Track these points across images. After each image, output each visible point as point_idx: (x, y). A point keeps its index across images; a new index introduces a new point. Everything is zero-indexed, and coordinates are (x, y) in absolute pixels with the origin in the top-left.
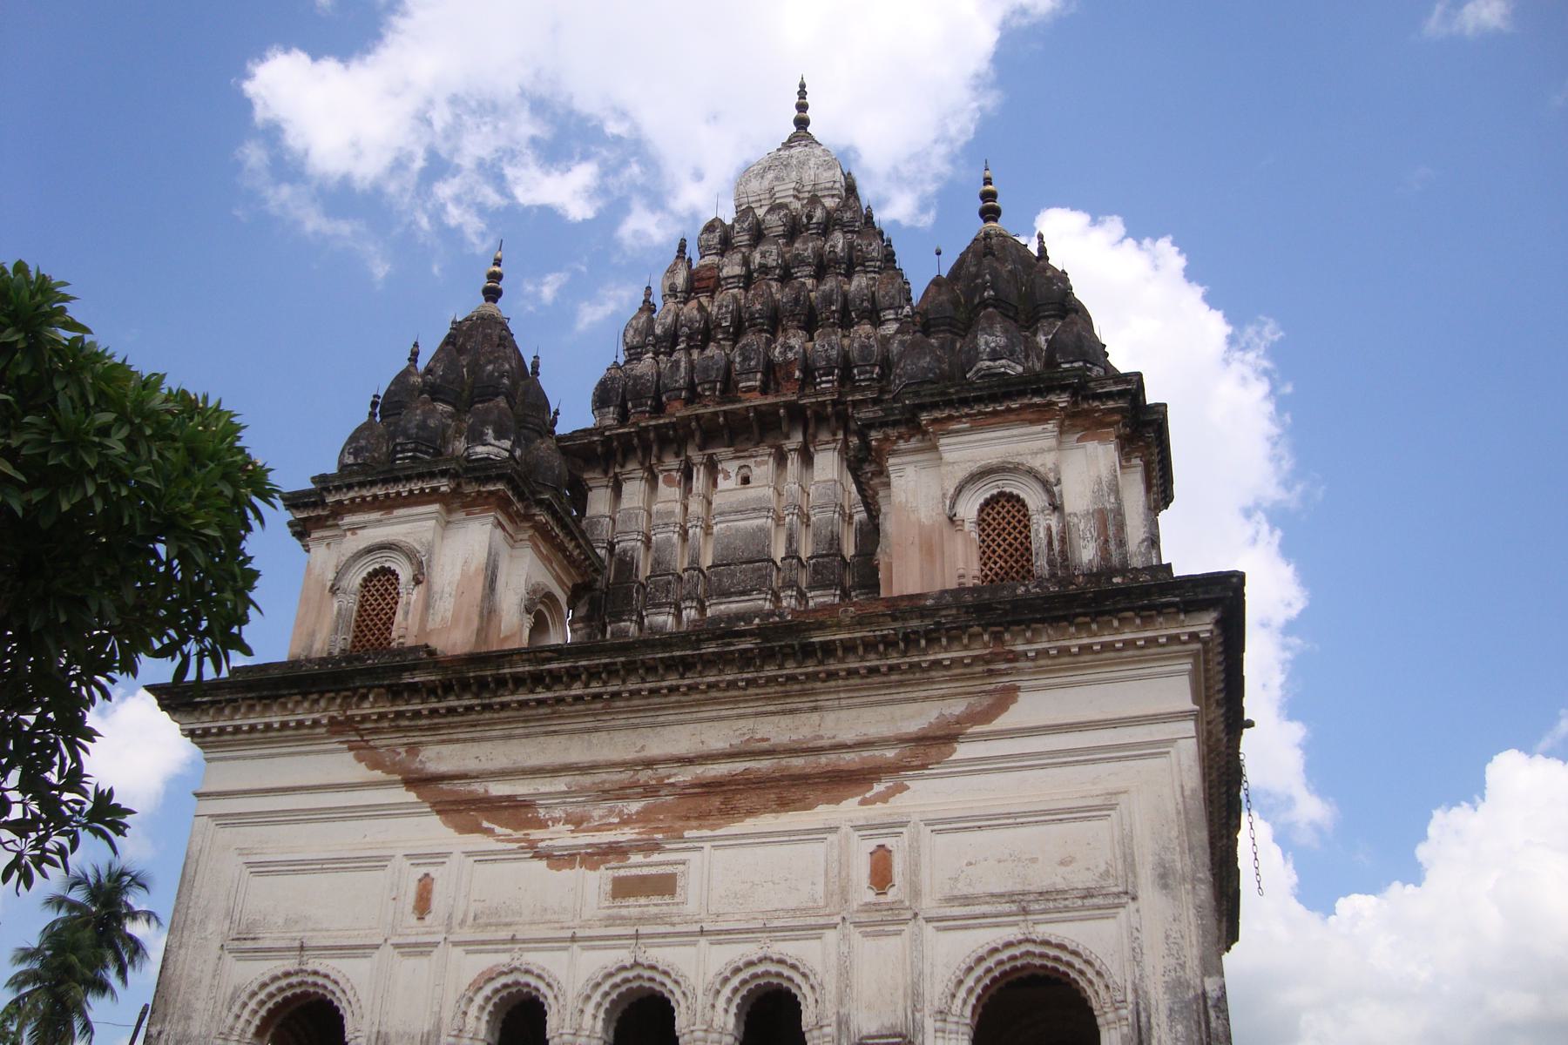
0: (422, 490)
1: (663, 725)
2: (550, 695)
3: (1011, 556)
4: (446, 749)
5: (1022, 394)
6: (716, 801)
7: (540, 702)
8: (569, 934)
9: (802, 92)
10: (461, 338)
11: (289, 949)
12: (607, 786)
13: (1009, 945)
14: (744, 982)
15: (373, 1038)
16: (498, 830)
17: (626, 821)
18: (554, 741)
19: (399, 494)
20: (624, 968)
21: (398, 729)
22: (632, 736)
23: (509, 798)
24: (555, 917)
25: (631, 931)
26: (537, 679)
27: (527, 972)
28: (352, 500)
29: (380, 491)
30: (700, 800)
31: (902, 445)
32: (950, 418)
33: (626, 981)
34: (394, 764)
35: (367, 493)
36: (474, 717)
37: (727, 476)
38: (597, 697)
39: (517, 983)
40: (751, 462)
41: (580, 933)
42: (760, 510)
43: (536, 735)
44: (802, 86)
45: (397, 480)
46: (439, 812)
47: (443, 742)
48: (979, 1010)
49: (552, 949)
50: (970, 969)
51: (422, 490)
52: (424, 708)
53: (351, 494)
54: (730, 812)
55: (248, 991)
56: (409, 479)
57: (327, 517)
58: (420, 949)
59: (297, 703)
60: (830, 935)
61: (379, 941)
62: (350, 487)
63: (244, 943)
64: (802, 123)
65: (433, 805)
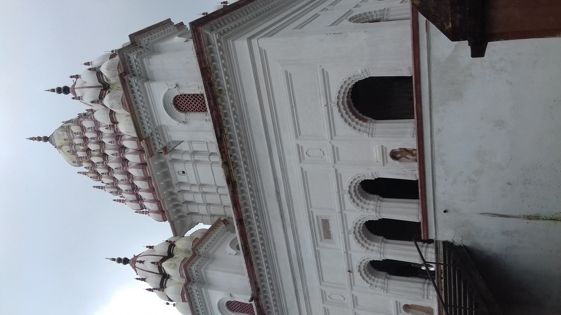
3: (197, 101)
9: (33, 139)
13: (340, 111)
14: (358, 198)
20: (356, 237)
27: (360, 266)
33: (360, 235)
39: (364, 269)
44: (31, 139)
48: (365, 117)
50: (349, 124)
60: (338, 172)
64: (46, 139)
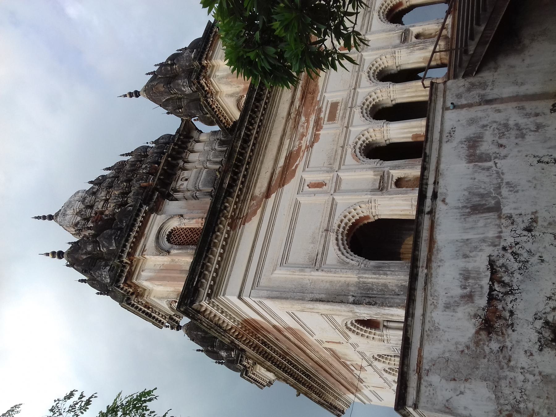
0: (143, 217)
1: (276, 113)
2: (252, 140)
4: (258, 185)
5: (209, 36)
6: (309, 96)
7: (254, 144)
8: (345, 129)
9: (38, 218)
10: (73, 263)
11: (326, 237)
12: (293, 126)
15: (372, 193)
16: (297, 163)
17: (308, 121)
18: (270, 146)
19: (139, 227)
21: (244, 201)
22: (277, 121)
23: (286, 158)
24: (337, 137)
25: (349, 109)
26: (246, 141)
28: (131, 247)
29: (133, 234)
30: (307, 100)
31: (208, 73)
32: (207, 55)
34: (257, 205)
35: (131, 239)
36: (250, 171)
37: (182, 184)
38: (259, 127)
40: (181, 177)
41: (346, 125)
42: (200, 171)
43: (265, 152)
44: (36, 218)
45: (133, 225)
46: (283, 186)
47: (255, 186)
49: (349, 135)
51: (143, 217)
52: (239, 186)
53: (128, 247)
54: (314, 92)
55: (341, 255)
56: (135, 220)
57: (130, 268)
58: (338, 181)
59: (217, 237)
61: (331, 197)
62: (125, 246)
63: (317, 262)
64: (51, 217)
65: (280, 187)
